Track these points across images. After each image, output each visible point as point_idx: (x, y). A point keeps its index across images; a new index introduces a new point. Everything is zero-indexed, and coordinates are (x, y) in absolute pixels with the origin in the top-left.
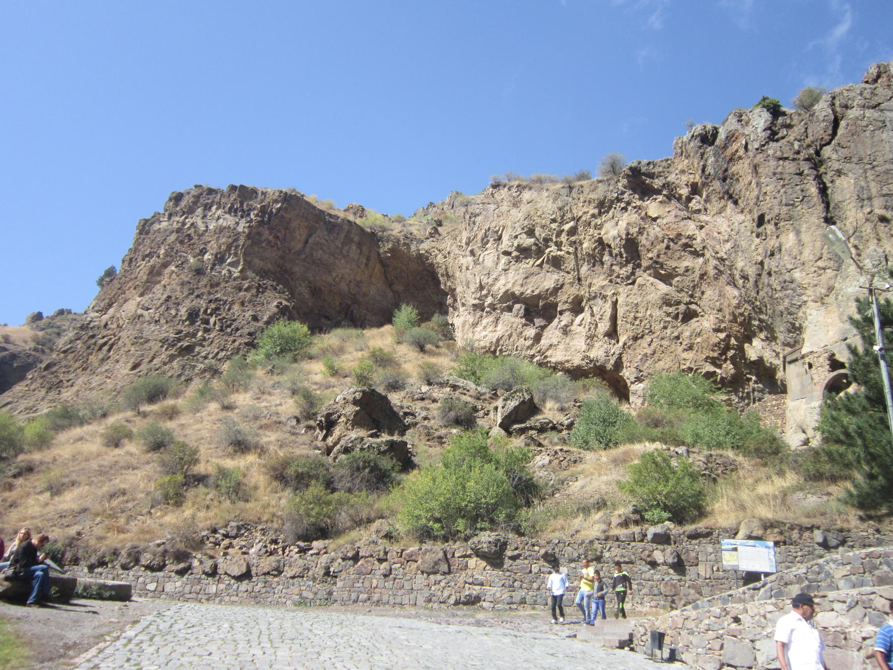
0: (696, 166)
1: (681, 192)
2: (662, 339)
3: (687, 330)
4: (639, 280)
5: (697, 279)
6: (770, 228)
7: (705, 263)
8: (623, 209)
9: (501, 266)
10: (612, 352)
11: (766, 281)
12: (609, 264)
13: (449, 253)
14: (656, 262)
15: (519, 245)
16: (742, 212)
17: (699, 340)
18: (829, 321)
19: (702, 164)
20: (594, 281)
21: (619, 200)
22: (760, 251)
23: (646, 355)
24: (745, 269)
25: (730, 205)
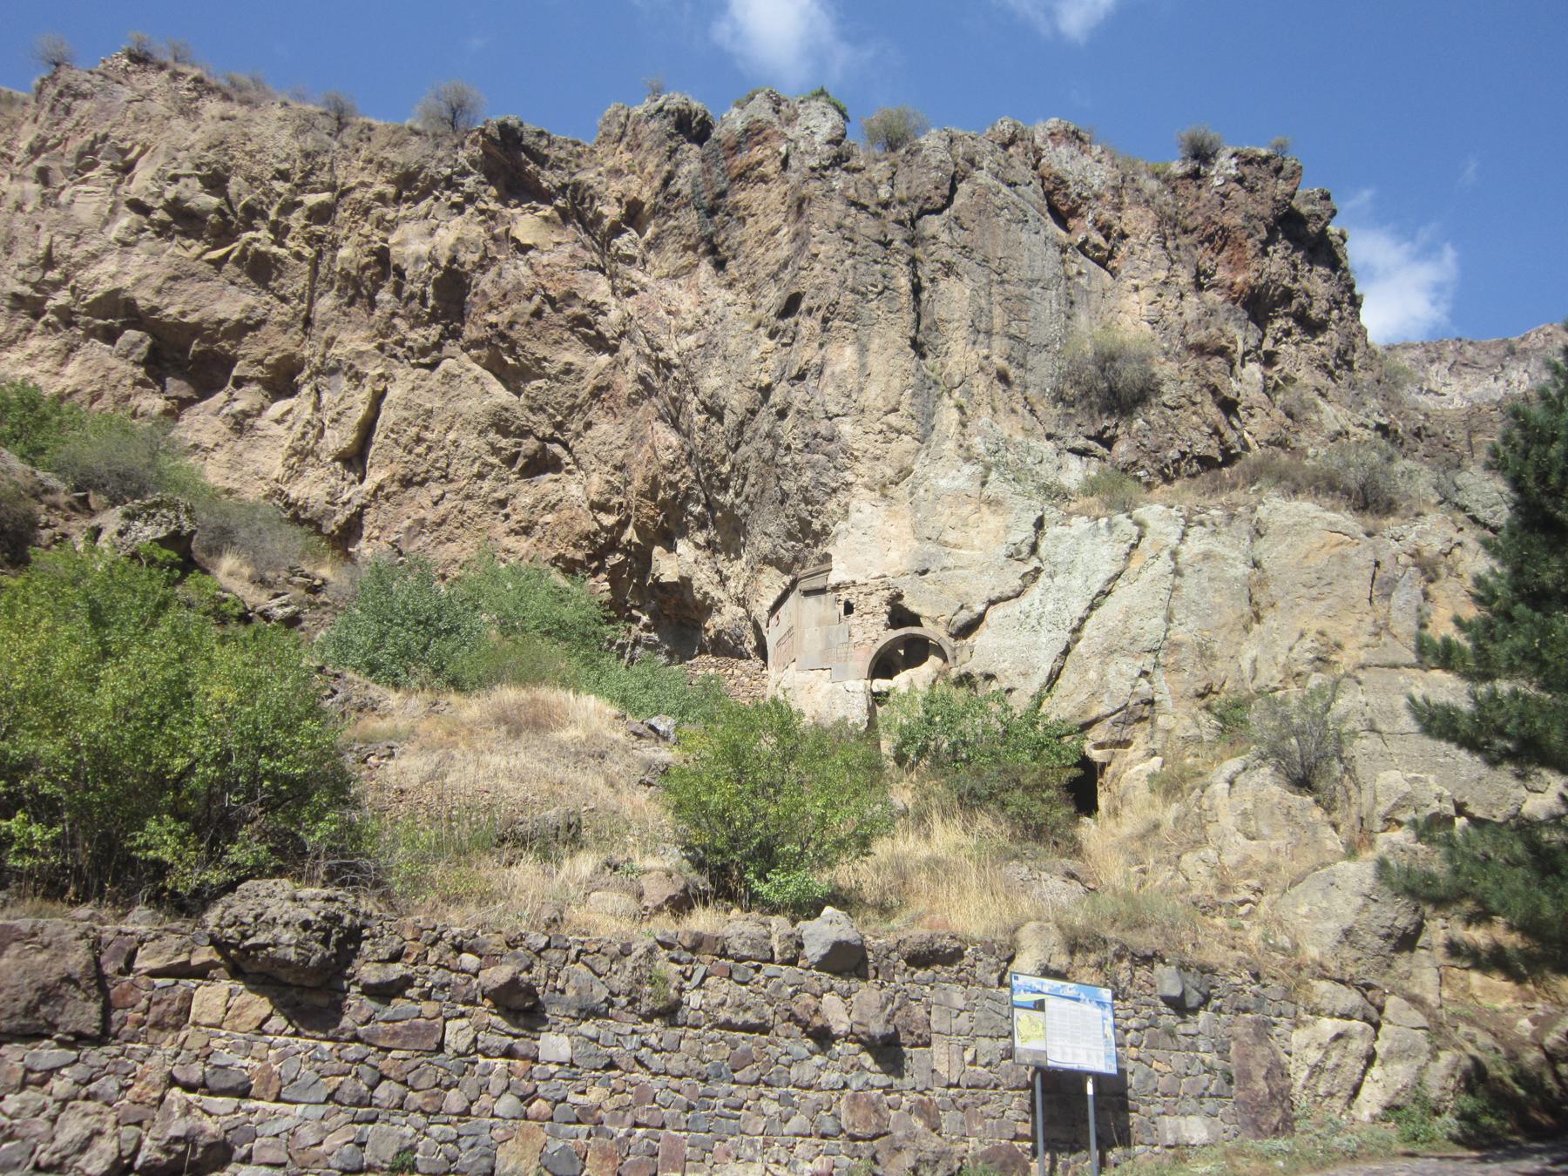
0: (650, 168)
1: (605, 210)
2: (468, 497)
3: (527, 494)
5: (583, 395)
8: (454, 205)
9: (115, 231)
10: (345, 497)
11: (766, 427)
12: (388, 309)
14: (503, 337)
15: (176, 200)
16: (730, 285)
17: (549, 518)
19: (667, 167)
20: (343, 336)
21: (450, 184)
23: (421, 522)
24: (723, 393)
25: (705, 267)
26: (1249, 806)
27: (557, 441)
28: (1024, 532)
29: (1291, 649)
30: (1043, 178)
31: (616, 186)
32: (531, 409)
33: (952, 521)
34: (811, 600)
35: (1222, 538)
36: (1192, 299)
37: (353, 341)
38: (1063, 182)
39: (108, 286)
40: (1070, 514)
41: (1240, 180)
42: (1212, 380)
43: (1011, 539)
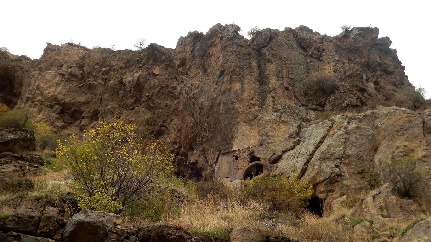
5: (170, 112)
7: (178, 103)
8: (139, 67)
11: (216, 110)
12: (122, 96)
13: (27, 71)
14: (149, 99)
15: (71, 72)
22: (216, 92)
26: (382, 204)
27: (164, 126)
28: (294, 129)
29: (394, 152)
30: (298, 40)
32: (157, 118)
33: (271, 129)
35: (363, 123)
38: (304, 39)
39: (52, 94)
41: (359, 35)
43: (290, 132)
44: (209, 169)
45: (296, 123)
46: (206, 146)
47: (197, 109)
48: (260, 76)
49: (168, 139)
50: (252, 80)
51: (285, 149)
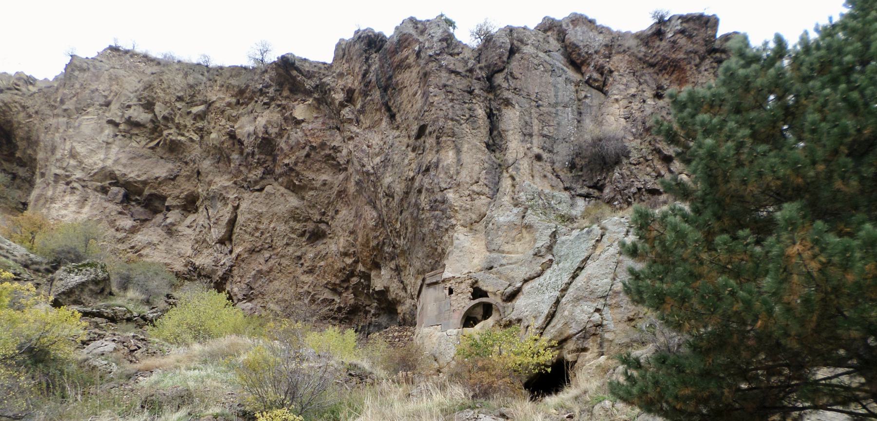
4: (268, 188)
5: (333, 196)
6: (430, 141)
7: (347, 179)
8: (265, 104)
11: (414, 200)
12: (237, 163)
13: (36, 113)
14: (291, 170)
15: (130, 117)
16: (398, 128)
17: (322, 263)
18: (475, 248)
20: (217, 179)
22: (413, 166)
24: (393, 185)
27: (324, 222)
28: (544, 241)
31: (341, 83)
32: (310, 207)
34: (431, 290)
36: (650, 102)
37: (221, 182)
38: (577, 47)
40: (572, 229)
42: (658, 146)
43: (537, 245)
44: (409, 302)
45: (548, 227)
46: (402, 262)
47: (381, 195)
48: (491, 134)
49: (333, 247)
50: (476, 145)
51: (528, 275)
